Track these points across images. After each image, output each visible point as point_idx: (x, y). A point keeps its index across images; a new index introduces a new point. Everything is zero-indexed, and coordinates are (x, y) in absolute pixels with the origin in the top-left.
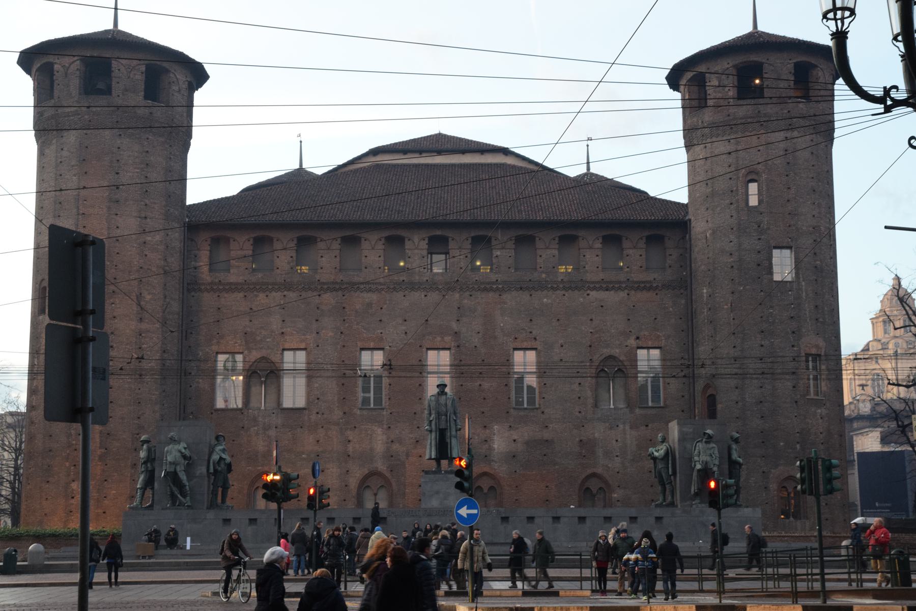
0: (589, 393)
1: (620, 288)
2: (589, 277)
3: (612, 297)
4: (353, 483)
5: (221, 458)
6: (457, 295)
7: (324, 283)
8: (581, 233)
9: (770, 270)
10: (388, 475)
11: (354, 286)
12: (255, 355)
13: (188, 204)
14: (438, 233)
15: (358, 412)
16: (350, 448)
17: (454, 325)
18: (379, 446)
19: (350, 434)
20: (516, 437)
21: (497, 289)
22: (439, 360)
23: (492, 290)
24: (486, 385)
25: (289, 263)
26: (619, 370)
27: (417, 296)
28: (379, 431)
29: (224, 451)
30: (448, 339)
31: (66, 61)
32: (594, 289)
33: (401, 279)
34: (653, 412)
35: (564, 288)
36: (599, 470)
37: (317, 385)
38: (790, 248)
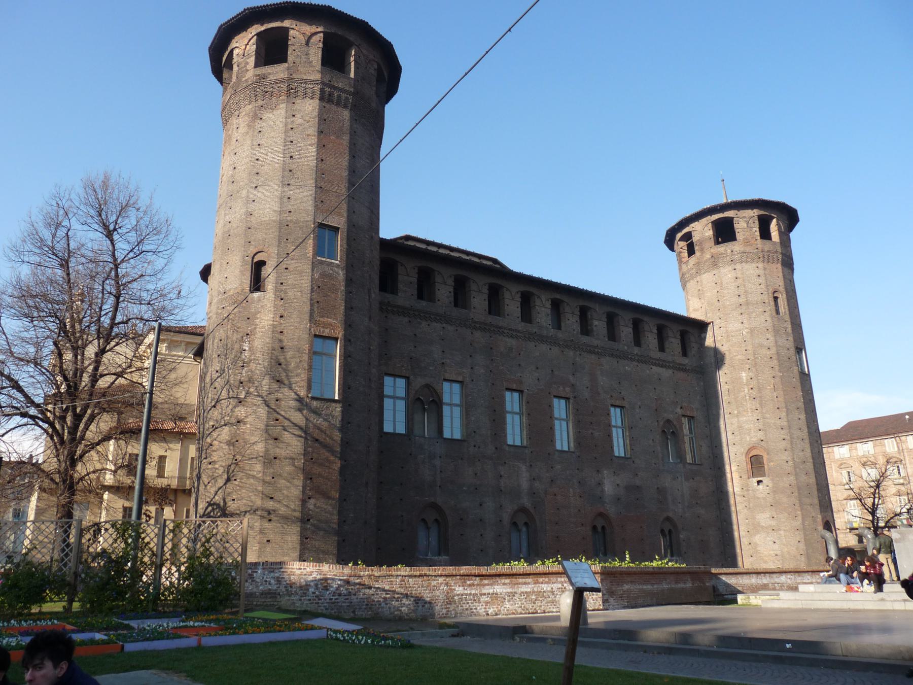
1: (669, 367)
3: (666, 373)
4: (506, 519)
6: (571, 353)
7: (476, 322)
8: (646, 319)
10: (532, 511)
12: (419, 382)
14: (558, 296)
15: (507, 448)
17: (571, 378)
18: (525, 484)
20: (618, 482)
21: (598, 353)
22: (560, 408)
23: (594, 353)
24: (596, 434)
25: (448, 297)
26: (673, 432)
27: (544, 347)
28: (524, 468)
30: (568, 389)
32: (655, 365)
33: (535, 330)
34: (695, 468)
35: (638, 361)
36: (671, 515)
37: (473, 418)
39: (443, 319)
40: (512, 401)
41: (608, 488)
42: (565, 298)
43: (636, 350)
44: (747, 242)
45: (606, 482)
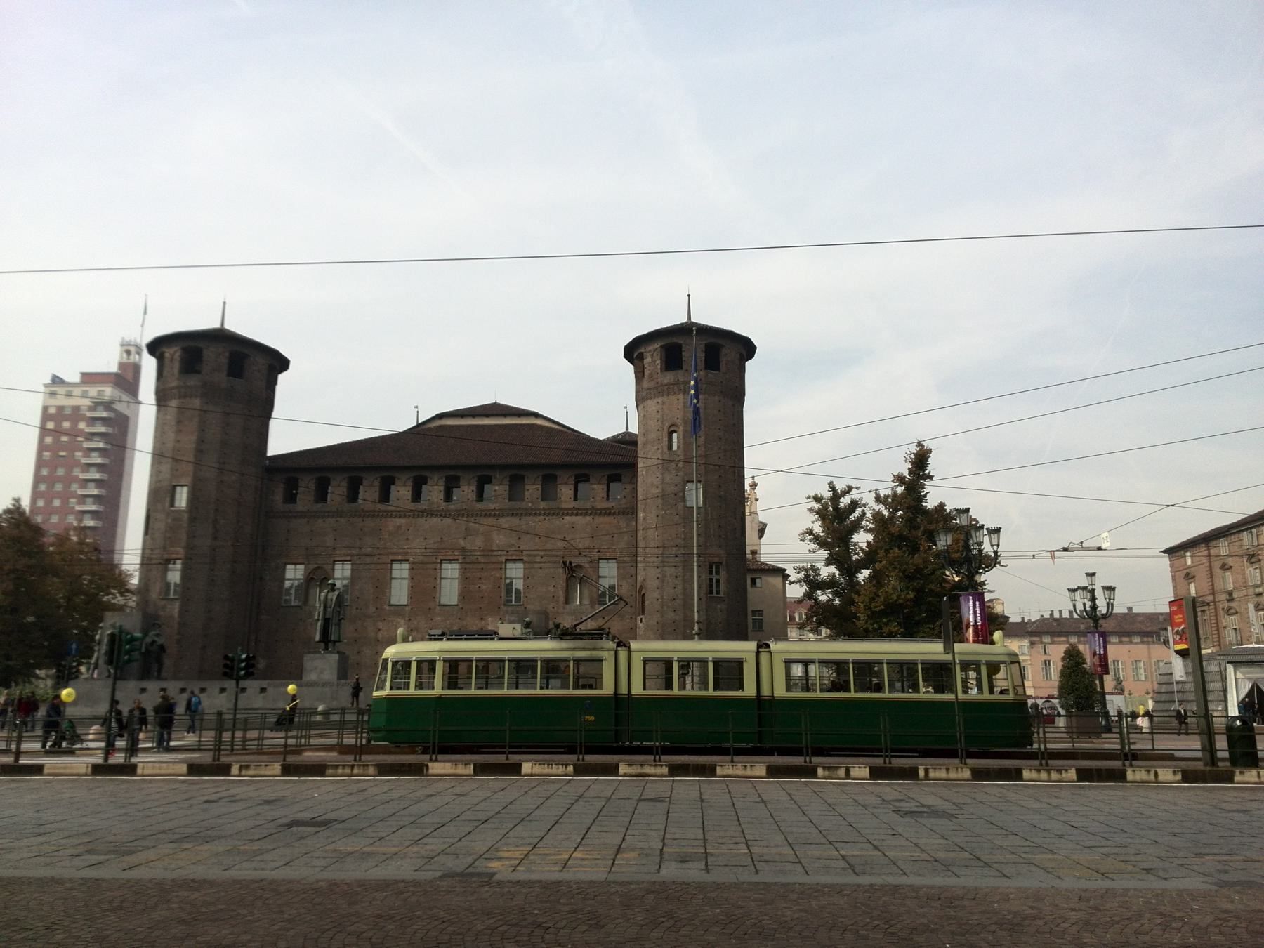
0: (561, 593)
1: (586, 514)
2: (564, 506)
5: (154, 642)
8: (558, 473)
9: (684, 499)
11: (389, 514)
13: (270, 453)
14: (452, 473)
16: (380, 636)
17: (462, 542)
19: (380, 625)
22: (451, 571)
24: (484, 587)
27: (436, 520)
29: (157, 635)
31: (172, 350)
39: (339, 514)
40: (401, 571)
42: (459, 474)
43: (543, 505)
44: (651, 377)
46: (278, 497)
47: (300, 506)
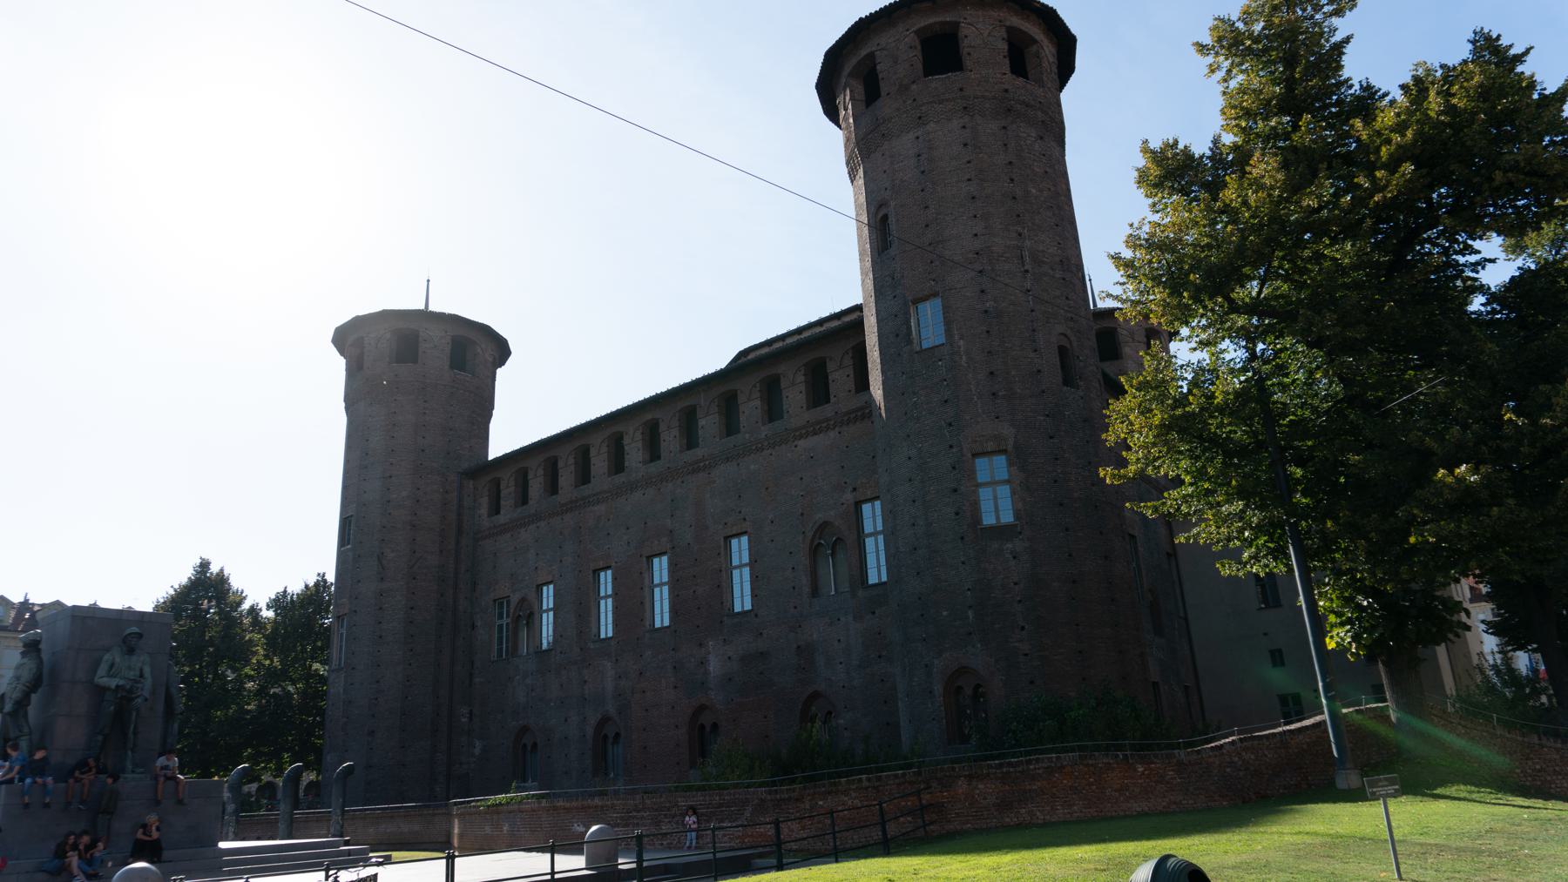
1: (828, 428)
14: (649, 416)
32: (801, 437)
38: (935, 295)
41: (714, 666)
43: (765, 431)
45: (712, 658)
46: (484, 511)
47: (502, 518)
